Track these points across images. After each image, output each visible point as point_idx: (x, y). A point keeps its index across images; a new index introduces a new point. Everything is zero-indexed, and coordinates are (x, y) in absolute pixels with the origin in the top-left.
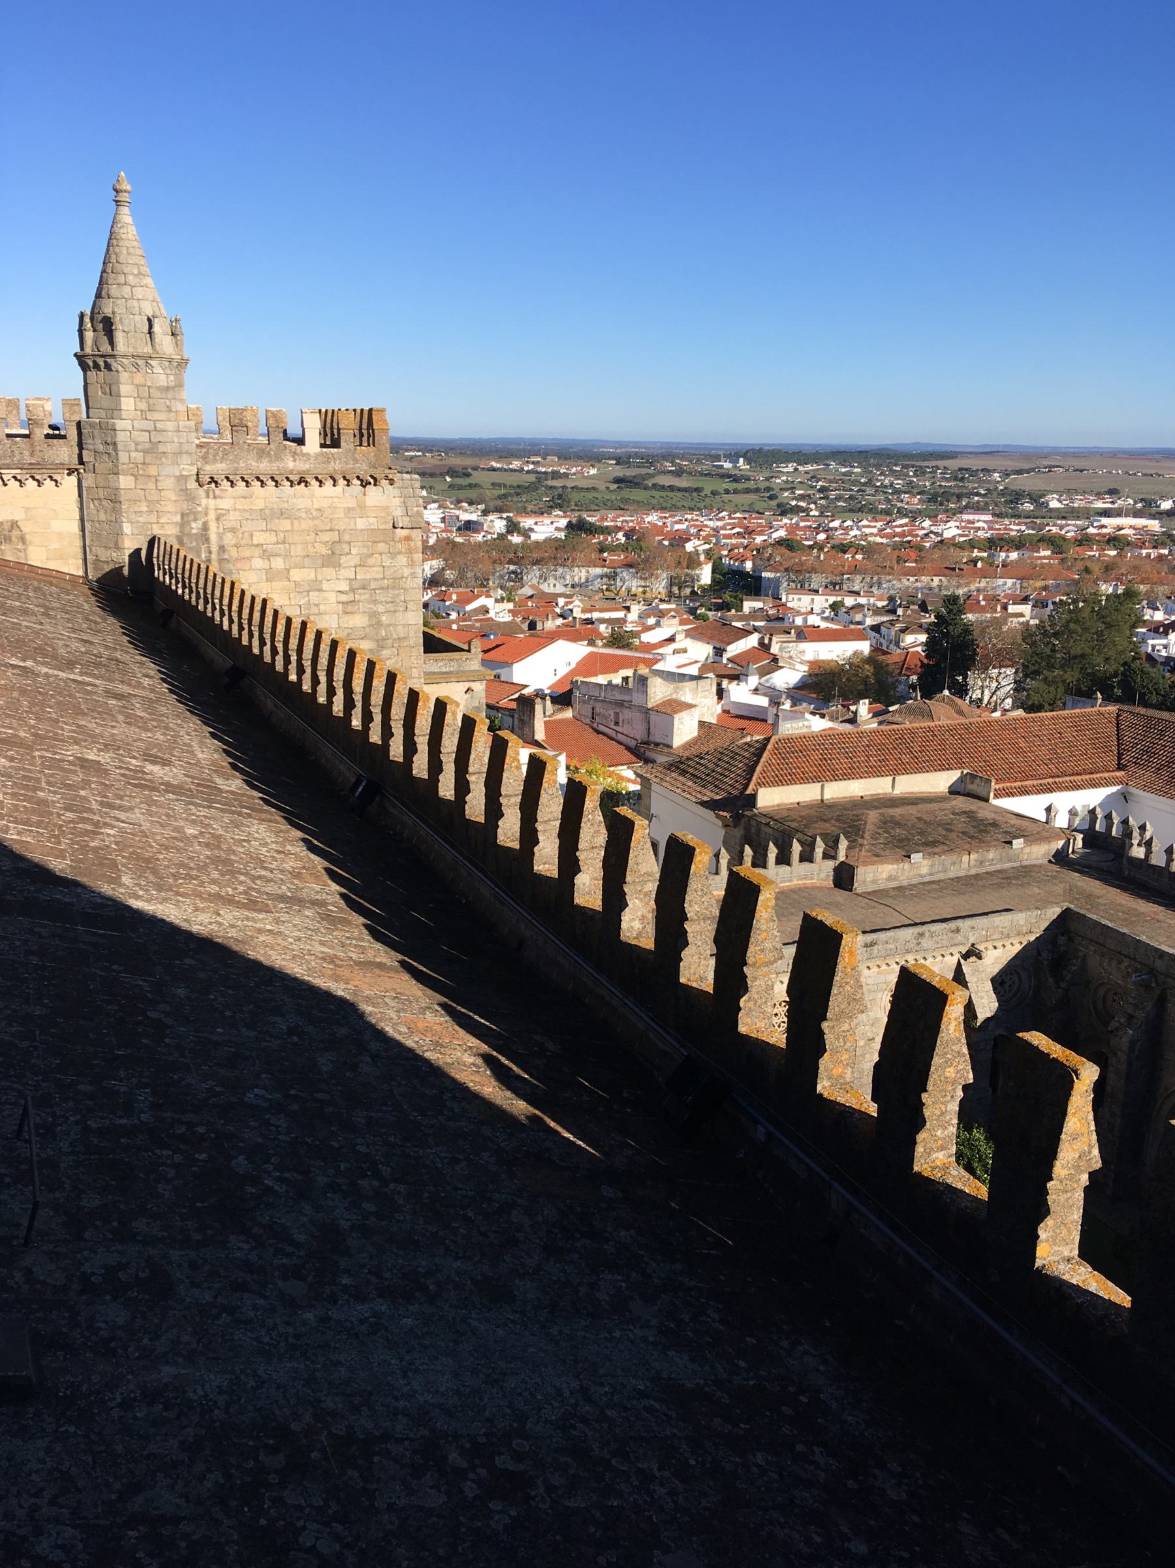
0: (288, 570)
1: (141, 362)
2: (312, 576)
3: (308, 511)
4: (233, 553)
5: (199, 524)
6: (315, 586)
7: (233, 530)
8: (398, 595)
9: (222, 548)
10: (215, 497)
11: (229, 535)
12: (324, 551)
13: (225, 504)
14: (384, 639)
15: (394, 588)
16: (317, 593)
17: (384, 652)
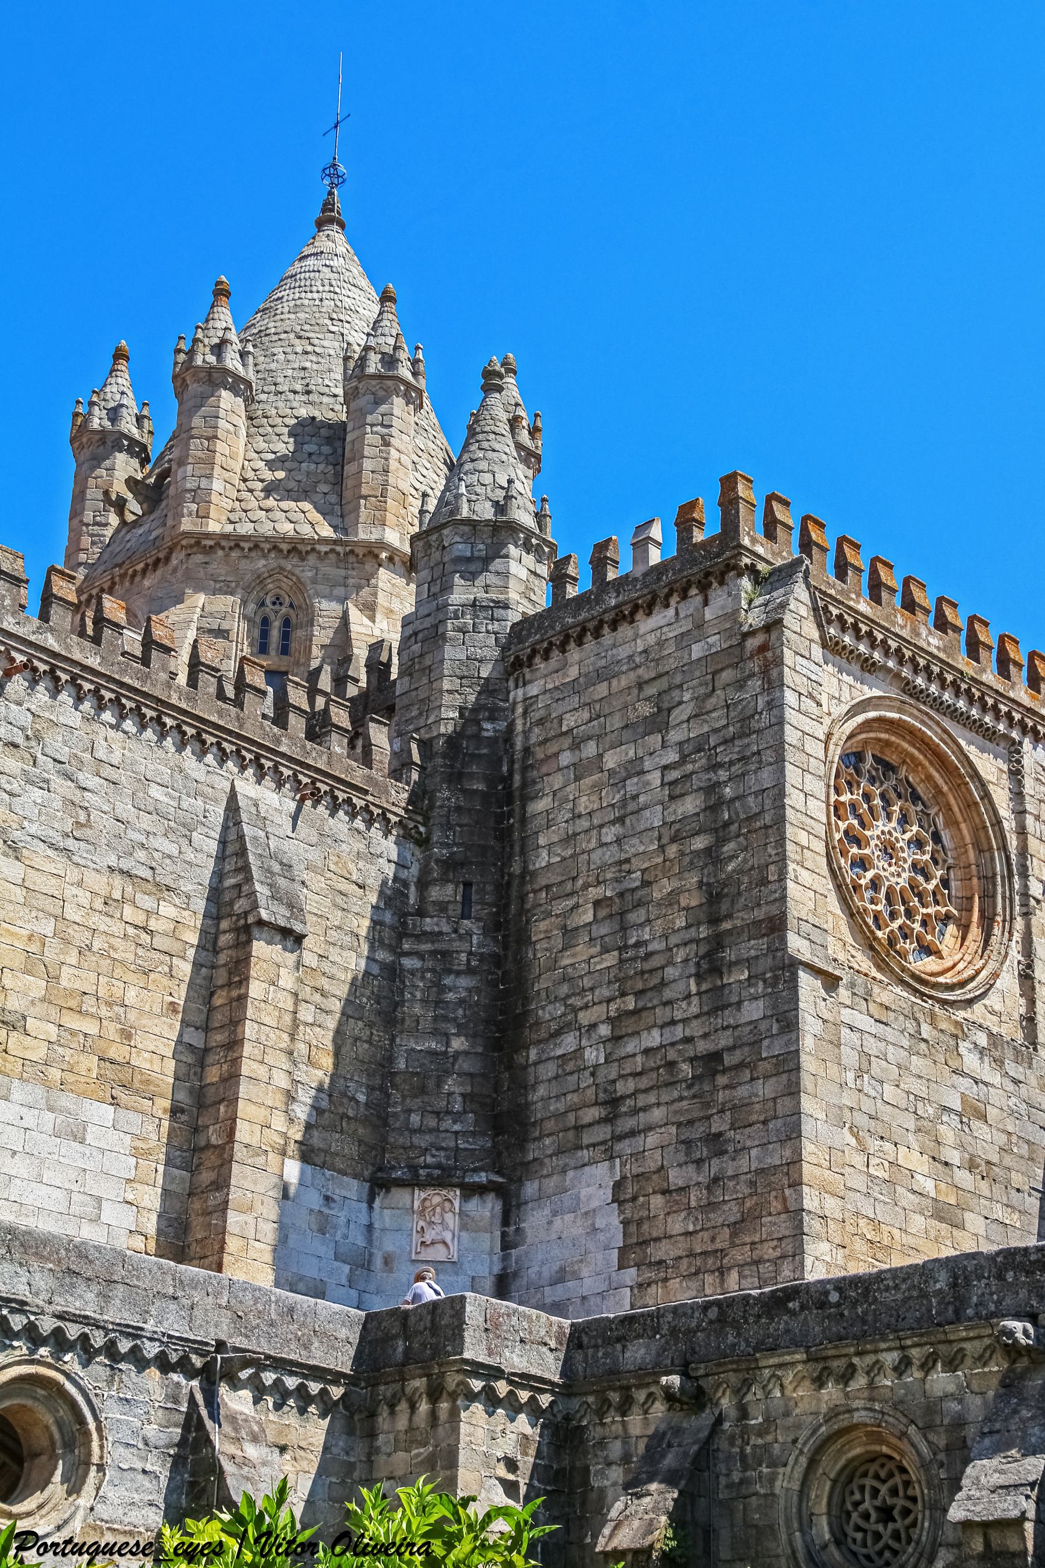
0: (600, 756)
1: (434, 537)
2: (631, 753)
3: (630, 657)
4: (540, 755)
5: (502, 725)
6: (634, 769)
7: (541, 722)
8: (748, 745)
9: (527, 751)
10: (524, 685)
11: (536, 730)
12: (646, 709)
13: (533, 690)
14: (726, 825)
15: (742, 735)
16: (635, 780)
17: (725, 849)
